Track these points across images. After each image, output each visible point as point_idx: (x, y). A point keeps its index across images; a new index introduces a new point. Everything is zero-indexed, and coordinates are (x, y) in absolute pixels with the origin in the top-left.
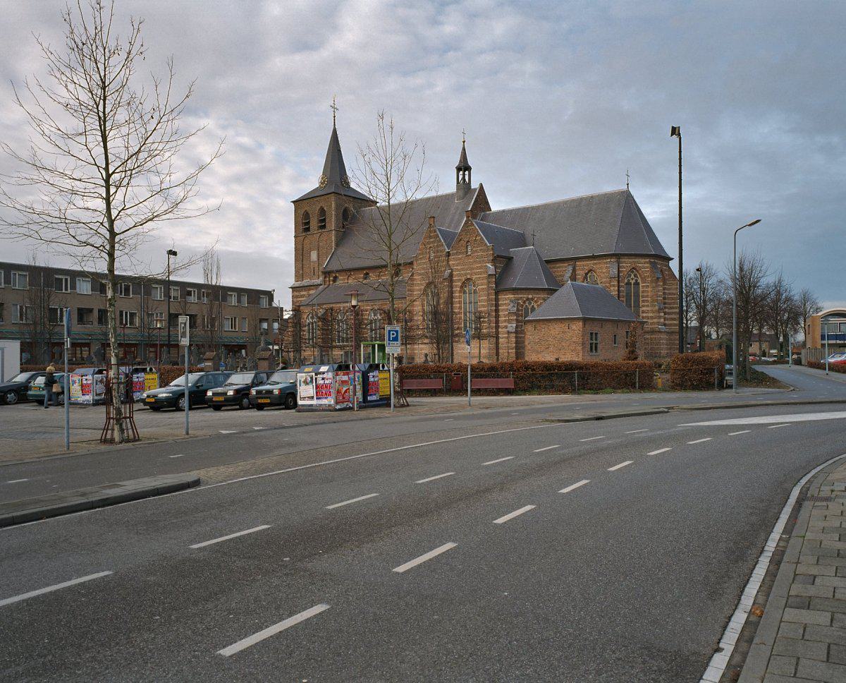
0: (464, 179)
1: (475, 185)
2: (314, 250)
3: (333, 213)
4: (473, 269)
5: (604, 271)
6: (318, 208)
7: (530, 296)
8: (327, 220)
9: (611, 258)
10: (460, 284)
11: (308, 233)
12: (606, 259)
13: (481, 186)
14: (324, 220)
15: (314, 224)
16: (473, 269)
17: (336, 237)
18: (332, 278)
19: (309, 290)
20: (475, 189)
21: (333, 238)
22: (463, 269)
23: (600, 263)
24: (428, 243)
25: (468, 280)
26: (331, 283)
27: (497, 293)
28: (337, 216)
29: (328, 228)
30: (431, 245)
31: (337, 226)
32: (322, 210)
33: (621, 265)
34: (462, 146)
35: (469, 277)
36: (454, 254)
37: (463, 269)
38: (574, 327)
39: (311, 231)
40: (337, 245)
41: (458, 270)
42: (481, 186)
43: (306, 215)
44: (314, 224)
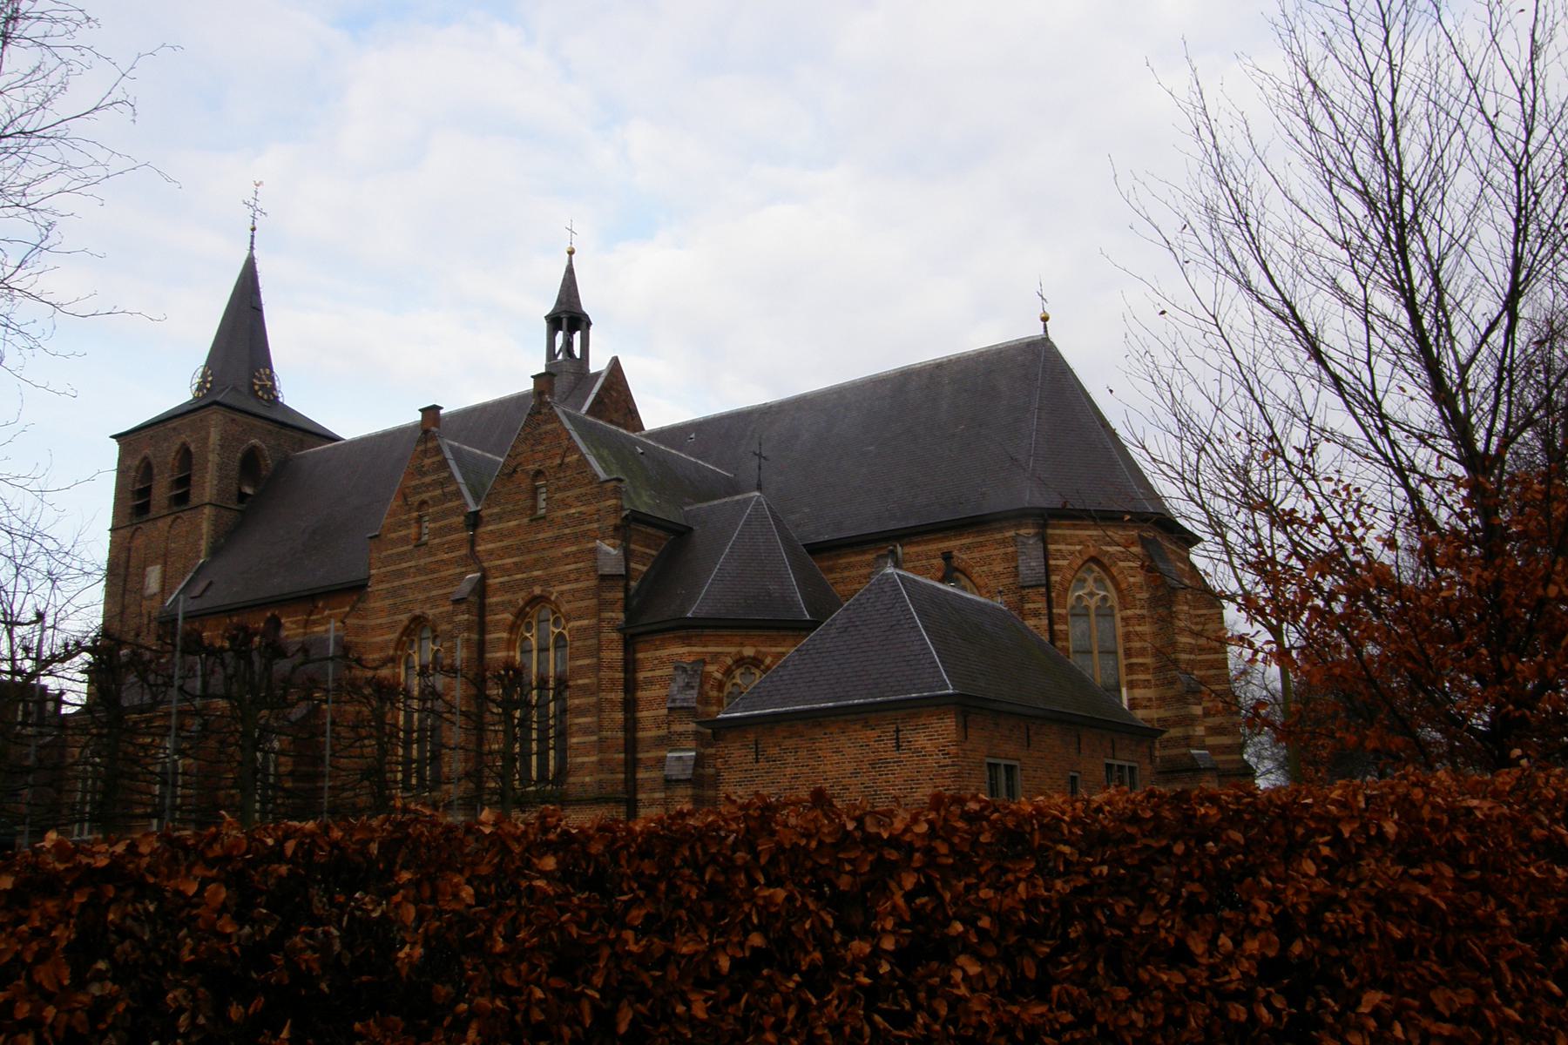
0: (568, 345)
1: (598, 363)
3: (211, 457)
4: (553, 562)
5: (998, 568)
6: (176, 447)
7: (749, 651)
8: (194, 478)
9: (1018, 527)
10: (508, 617)
11: (145, 518)
12: (1000, 530)
13: (615, 365)
15: (161, 492)
16: (553, 562)
20: (598, 374)
21: (205, 527)
22: (519, 568)
23: (981, 545)
25: (534, 601)
27: (631, 641)
28: (221, 467)
30: (425, 496)
32: (185, 454)
33: (1052, 547)
34: (566, 263)
35: (537, 590)
37: (519, 568)
38: (921, 740)
39: (153, 512)
40: (215, 551)
41: (504, 570)
42: (615, 365)
43: (147, 469)
44: (161, 492)
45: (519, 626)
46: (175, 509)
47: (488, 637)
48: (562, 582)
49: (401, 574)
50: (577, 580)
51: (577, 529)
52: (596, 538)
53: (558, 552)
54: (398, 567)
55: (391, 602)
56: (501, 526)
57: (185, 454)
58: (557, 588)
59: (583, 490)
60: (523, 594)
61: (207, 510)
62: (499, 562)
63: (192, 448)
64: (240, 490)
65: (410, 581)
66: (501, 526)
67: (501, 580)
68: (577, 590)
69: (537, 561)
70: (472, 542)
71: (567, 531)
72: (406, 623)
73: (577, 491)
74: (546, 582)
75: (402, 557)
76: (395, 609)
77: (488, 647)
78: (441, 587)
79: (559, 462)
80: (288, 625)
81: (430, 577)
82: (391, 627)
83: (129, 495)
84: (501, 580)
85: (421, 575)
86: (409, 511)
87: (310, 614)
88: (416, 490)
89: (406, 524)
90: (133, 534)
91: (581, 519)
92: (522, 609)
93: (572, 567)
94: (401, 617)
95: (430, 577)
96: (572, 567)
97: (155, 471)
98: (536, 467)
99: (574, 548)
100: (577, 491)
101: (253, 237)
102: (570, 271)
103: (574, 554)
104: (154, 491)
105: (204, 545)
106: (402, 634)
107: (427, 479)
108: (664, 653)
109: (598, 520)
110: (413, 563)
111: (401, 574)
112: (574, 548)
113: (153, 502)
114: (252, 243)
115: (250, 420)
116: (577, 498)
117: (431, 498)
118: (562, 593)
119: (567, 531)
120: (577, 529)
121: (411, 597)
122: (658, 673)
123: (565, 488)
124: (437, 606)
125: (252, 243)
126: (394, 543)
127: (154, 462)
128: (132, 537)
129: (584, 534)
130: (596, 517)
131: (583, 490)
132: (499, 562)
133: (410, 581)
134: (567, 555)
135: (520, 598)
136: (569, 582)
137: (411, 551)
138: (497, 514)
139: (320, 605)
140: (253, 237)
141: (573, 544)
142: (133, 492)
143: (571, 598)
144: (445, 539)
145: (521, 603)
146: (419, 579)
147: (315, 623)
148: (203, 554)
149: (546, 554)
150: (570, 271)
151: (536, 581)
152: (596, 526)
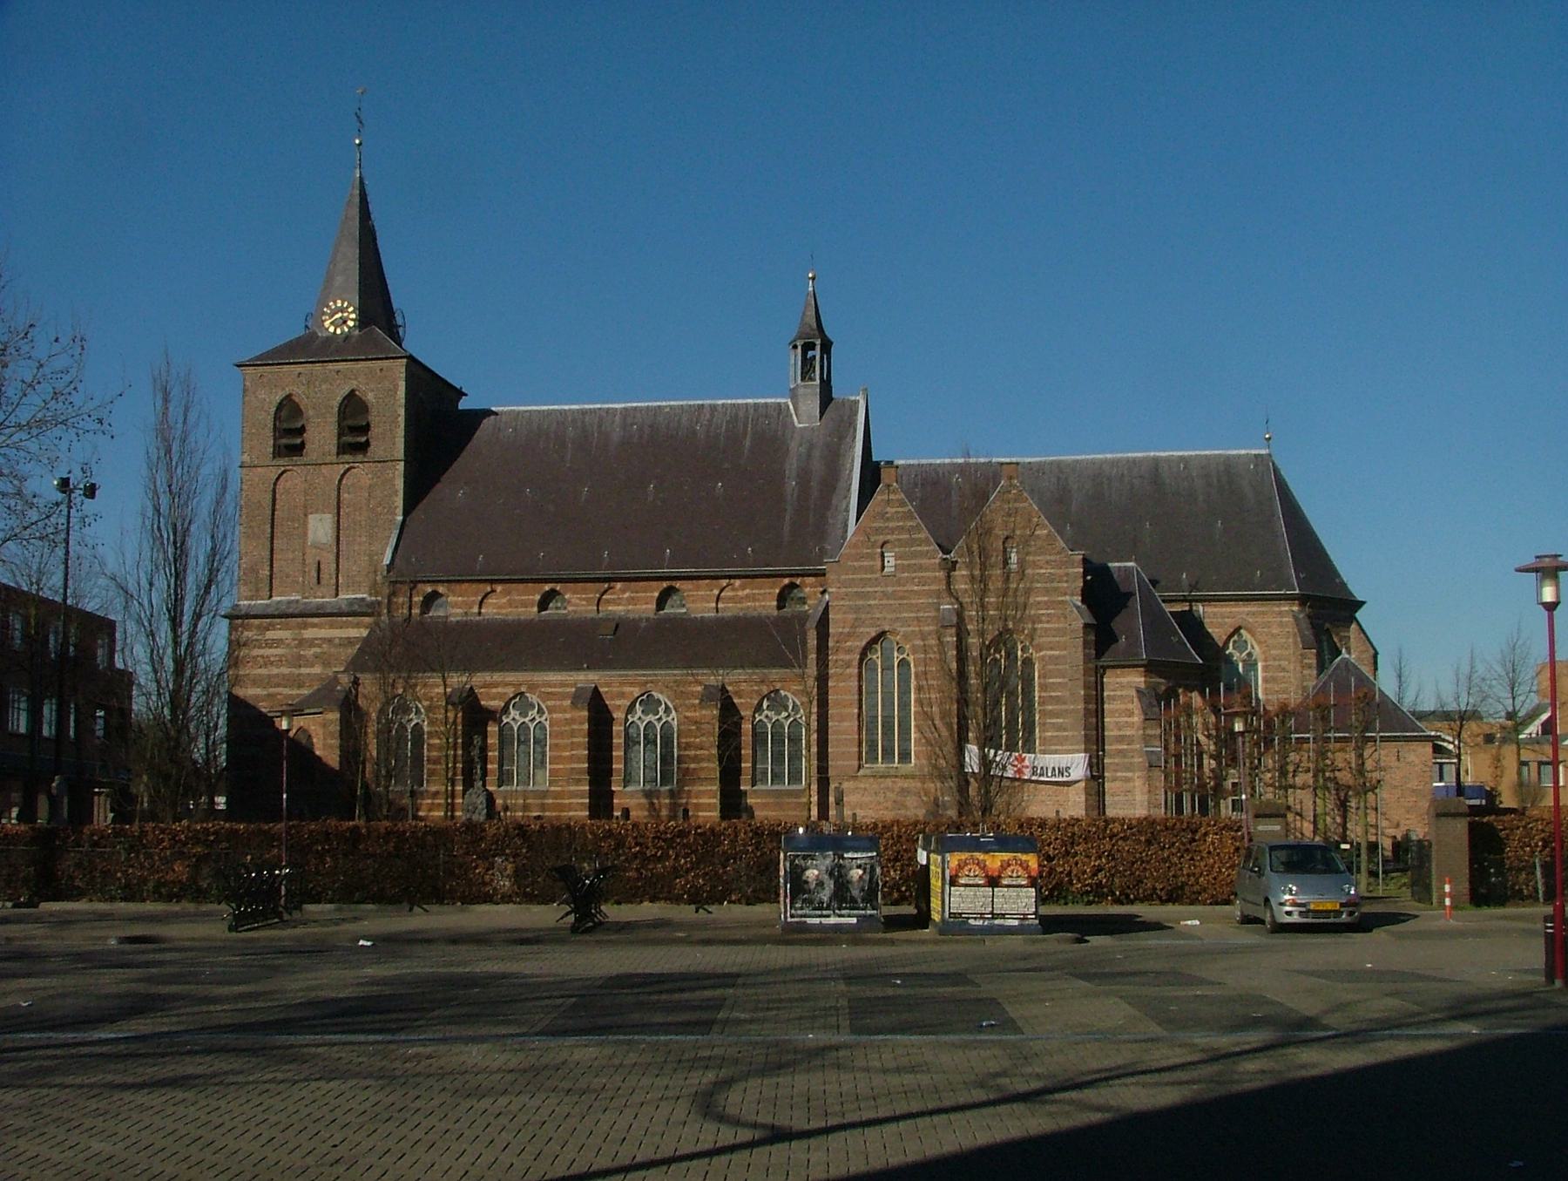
6: (346, 391)
8: (375, 431)
15: (322, 434)
21: (400, 484)
24: (878, 531)
29: (376, 449)
38: (1412, 757)
44: (322, 434)
46: (347, 457)
49: (865, 596)
50: (1048, 622)
51: (1048, 585)
59: (1052, 558)
63: (370, 397)
65: (876, 602)
68: (1050, 629)
75: (865, 583)
85: (888, 599)
88: (878, 531)
89: (870, 557)
94: (868, 630)
97: (311, 413)
99: (1046, 599)
100: (1048, 558)
103: (1046, 602)
105: (399, 501)
107: (891, 525)
108: (1124, 680)
109: (1067, 582)
111: (865, 596)
112: (1046, 599)
116: (1047, 562)
120: (1048, 585)
122: (1119, 693)
126: (855, 570)
127: (304, 403)
130: (1065, 579)
131: (1052, 558)
133: (876, 602)
144: (914, 575)
146: (884, 602)
147: (608, 602)
152: (1065, 585)
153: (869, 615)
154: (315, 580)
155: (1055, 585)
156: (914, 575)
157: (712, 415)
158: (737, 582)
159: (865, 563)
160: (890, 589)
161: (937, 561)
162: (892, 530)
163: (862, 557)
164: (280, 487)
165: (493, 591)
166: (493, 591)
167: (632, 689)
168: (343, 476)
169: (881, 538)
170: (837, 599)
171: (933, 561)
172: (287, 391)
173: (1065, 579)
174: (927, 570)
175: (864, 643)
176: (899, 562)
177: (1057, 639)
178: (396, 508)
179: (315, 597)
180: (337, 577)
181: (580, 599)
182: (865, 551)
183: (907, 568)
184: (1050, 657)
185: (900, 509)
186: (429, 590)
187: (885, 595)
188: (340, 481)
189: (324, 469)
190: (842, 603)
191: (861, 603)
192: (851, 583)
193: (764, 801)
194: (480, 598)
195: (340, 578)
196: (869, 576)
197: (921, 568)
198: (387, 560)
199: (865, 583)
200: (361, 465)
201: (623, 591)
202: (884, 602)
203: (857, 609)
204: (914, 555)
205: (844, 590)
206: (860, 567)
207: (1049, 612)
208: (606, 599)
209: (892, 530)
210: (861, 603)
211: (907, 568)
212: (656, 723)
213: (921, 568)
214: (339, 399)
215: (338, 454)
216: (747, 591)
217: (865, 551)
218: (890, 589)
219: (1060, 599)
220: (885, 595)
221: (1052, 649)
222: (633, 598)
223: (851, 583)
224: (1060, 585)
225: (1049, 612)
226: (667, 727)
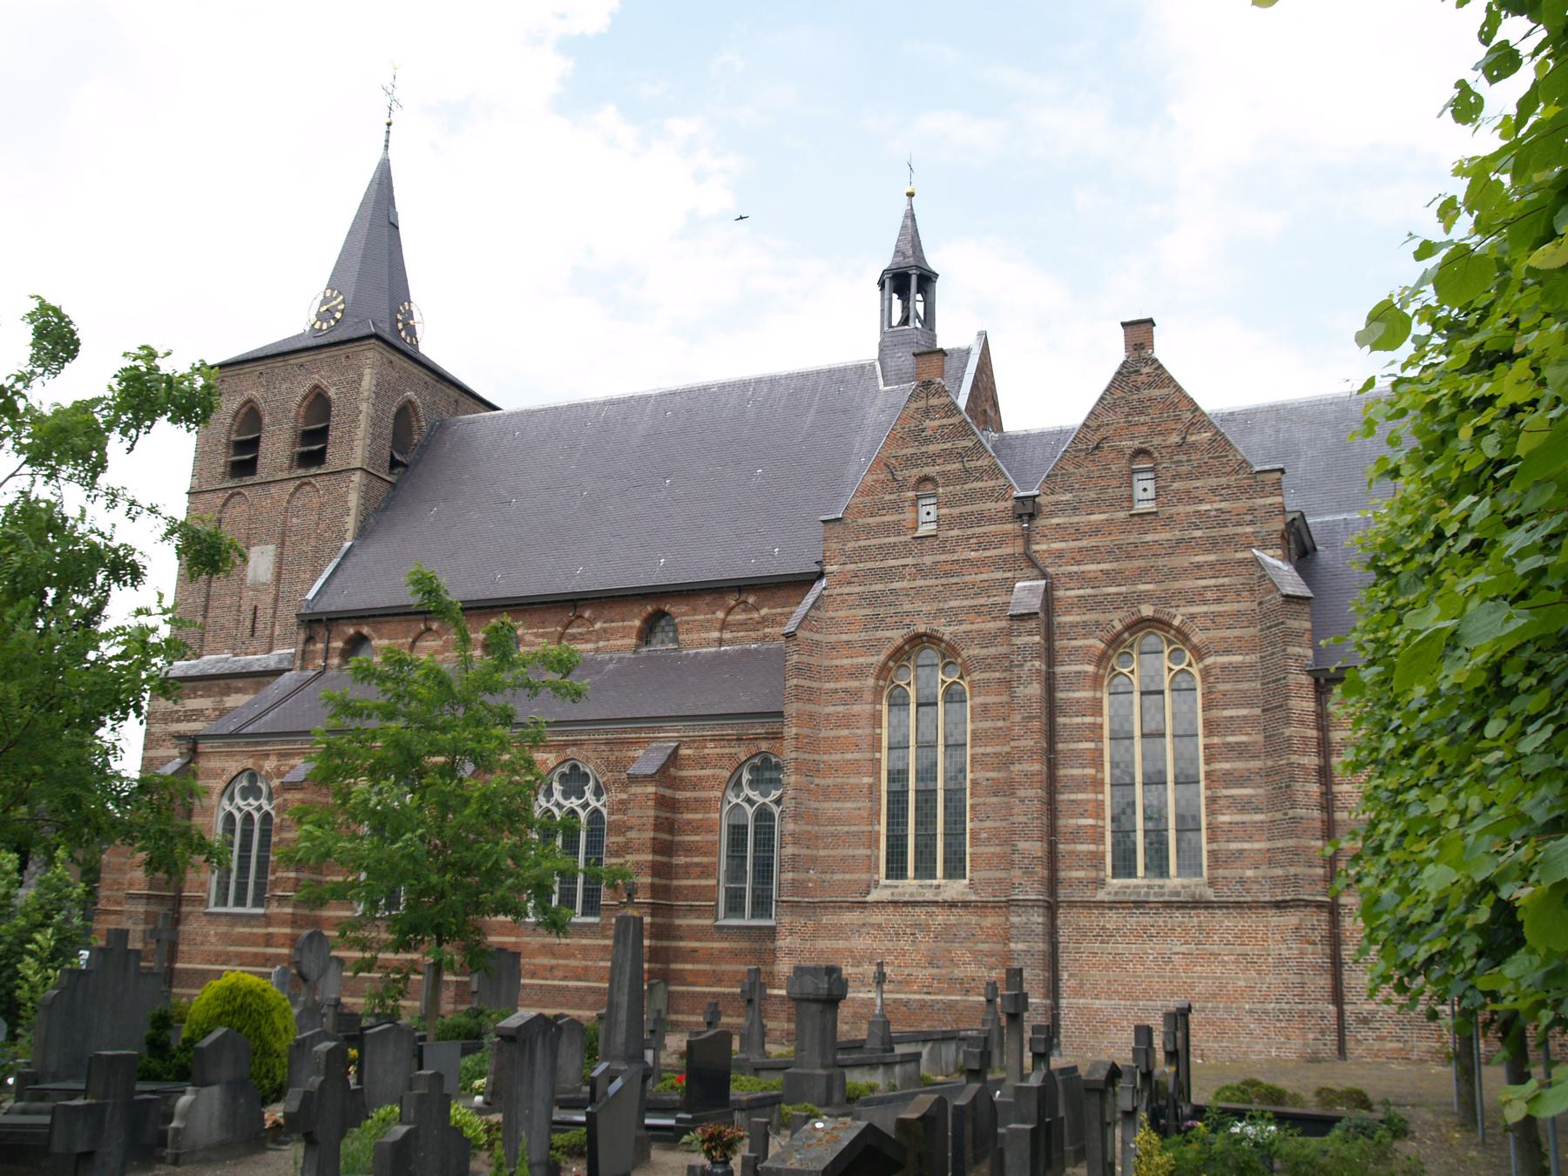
2: (261, 542)
3: (364, 407)
4: (1174, 574)
6: (303, 389)
8: (333, 434)
11: (248, 480)
14: (321, 435)
15: (276, 448)
16: (1174, 574)
17: (366, 497)
18: (338, 644)
19: (227, 691)
21: (353, 499)
22: (1111, 577)
24: (911, 461)
25: (1140, 625)
26: (335, 661)
28: (375, 422)
29: (335, 457)
30: (929, 471)
31: (373, 455)
32: (319, 403)
35: (1147, 611)
36: (1059, 510)
37: (1111, 577)
39: (263, 473)
40: (363, 532)
41: (1083, 579)
44: (276, 448)
45: (1109, 659)
46: (301, 472)
47: (1059, 669)
48: (1191, 602)
49: (886, 574)
50: (1219, 601)
51: (1214, 533)
52: (1249, 546)
53: (1181, 561)
54: (882, 564)
55: (868, 611)
56: (1075, 519)
57: (319, 403)
58: (1182, 610)
59: (1223, 480)
60: (1120, 614)
61: (357, 477)
62: (1075, 568)
63: (332, 393)
64: (392, 456)
65: (905, 584)
66: (1075, 519)
67: (1081, 592)
68: (1220, 614)
69: (1145, 570)
70: (1028, 539)
71: (1198, 533)
72: (900, 641)
73: (1213, 482)
74: (1165, 599)
75: (887, 551)
76: (876, 622)
77: (1060, 683)
78: (966, 597)
79: (1178, 439)
80: (529, 638)
81: (944, 581)
82: (871, 646)
83: (221, 449)
84: (1081, 592)
85: (924, 577)
86: (901, 488)
87: (567, 627)
88: (911, 461)
90: (228, 500)
91: (1221, 518)
92: (1119, 635)
93: (1212, 582)
94: (889, 634)
95: (944, 581)
96: (1212, 582)
97: (266, 420)
98: (1136, 444)
99: (1211, 558)
100: (1213, 482)
101: (388, 132)
102: (911, 216)
103: (1212, 565)
104: (264, 446)
105: (351, 523)
106: (890, 658)
107: (932, 448)
109: (1252, 523)
110: (910, 561)
111: (886, 574)
112: (1211, 558)
113: (261, 461)
114: (387, 141)
115: (408, 364)
116: (1213, 490)
117: (942, 474)
118: (1192, 617)
119: (1198, 533)
120: (1214, 533)
121: (907, 607)
123: (1189, 476)
124: (961, 622)
125: (387, 141)
126: (870, 531)
127: (263, 406)
128: (224, 505)
129: (1229, 540)
130: (1249, 518)
131: (1223, 480)
132: (1075, 568)
133: (905, 584)
134: (1199, 566)
135: (1117, 621)
136: (1205, 602)
137: (905, 544)
138: (1068, 503)
139: (587, 614)
140: (388, 132)
141: (1208, 551)
142: (228, 446)
143: (1209, 623)
144: (970, 532)
145: (1119, 626)
146: (920, 583)
147: (574, 638)
148: (349, 535)
149: (1160, 562)
150: (911, 216)
151: (1142, 598)
152: (1249, 529)
153: (892, 610)
154: (248, 632)
155: (1231, 530)
156: (970, 532)
157: (771, 391)
158: (751, 600)
159: (886, 519)
160: (928, 560)
161: (1010, 504)
162: (933, 459)
163: (882, 508)
164: (226, 516)
165: (429, 630)
166: (429, 630)
167: (545, 756)
168: (292, 495)
169: (916, 473)
170: (840, 583)
171: (1001, 505)
172: (246, 396)
173: (1249, 518)
174: (991, 520)
175: (882, 658)
176: (944, 511)
177: (1237, 632)
178: (346, 531)
179: (246, 654)
180: (273, 626)
181: (537, 635)
182: (887, 497)
183: (952, 522)
184: (1224, 668)
185: (945, 421)
186: (351, 631)
187: (920, 571)
188: (289, 502)
189: (274, 490)
190: (846, 590)
191: (879, 587)
192: (862, 554)
193: (734, 945)
194: (410, 640)
195: (277, 627)
196: (892, 540)
197: (981, 519)
198: (310, 596)
199: (887, 551)
200: (313, 481)
201: (591, 622)
202: (920, 583)
203: (872, 599)
204: (970, 497)
205: (852, 567)
206: (878, 525)
207: (1221, 581)
208: (571, 635)
209: (933, 459)
210: (879, 587)
211: (952, 522)
212: (580, 811)
213: (981, 519)
214: (299, 399)
215: (291, 467)
216: (764, 611)
217: (887, 497)
218: (928, 560)
219: (1240, 555)
220: (920, 571)
221: (1227, 652)
222: (605, 630)
223: (862, 554)
224: (1239, 530)
225: (1221, 581)
226: (596, 815)
